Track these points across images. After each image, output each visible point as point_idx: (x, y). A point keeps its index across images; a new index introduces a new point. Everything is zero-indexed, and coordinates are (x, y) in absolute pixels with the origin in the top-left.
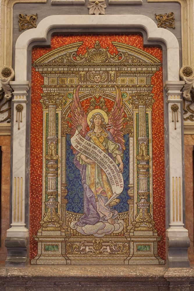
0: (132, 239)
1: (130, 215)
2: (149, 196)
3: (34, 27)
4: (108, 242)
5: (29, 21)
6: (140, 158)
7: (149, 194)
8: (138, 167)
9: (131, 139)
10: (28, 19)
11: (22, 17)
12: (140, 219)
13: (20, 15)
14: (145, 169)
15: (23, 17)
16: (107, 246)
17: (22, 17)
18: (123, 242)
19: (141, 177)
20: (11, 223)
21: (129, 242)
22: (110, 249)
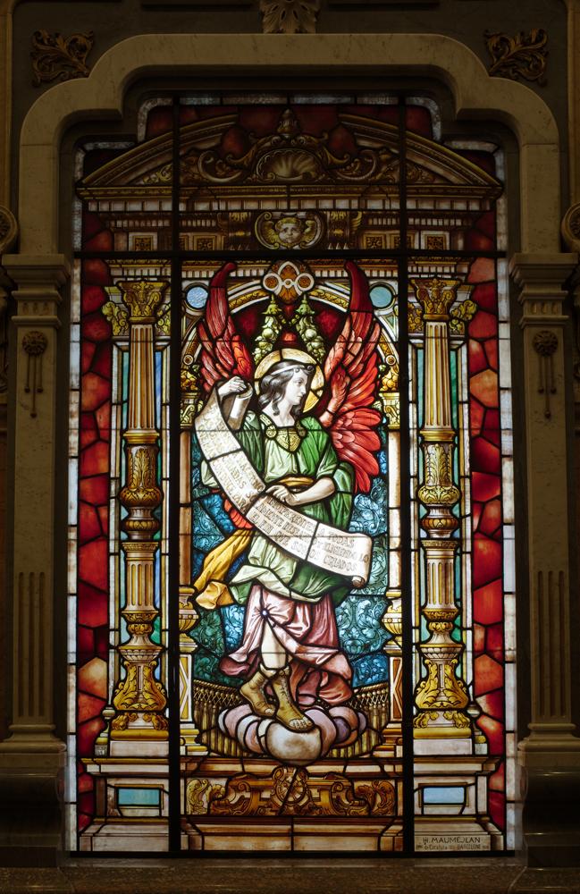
3: (82, 73)
5: (66, 52)
10: (62, 46)
11: (42, 42)
13: (38, 34)
15: (46, 42)
17: (42, 42)
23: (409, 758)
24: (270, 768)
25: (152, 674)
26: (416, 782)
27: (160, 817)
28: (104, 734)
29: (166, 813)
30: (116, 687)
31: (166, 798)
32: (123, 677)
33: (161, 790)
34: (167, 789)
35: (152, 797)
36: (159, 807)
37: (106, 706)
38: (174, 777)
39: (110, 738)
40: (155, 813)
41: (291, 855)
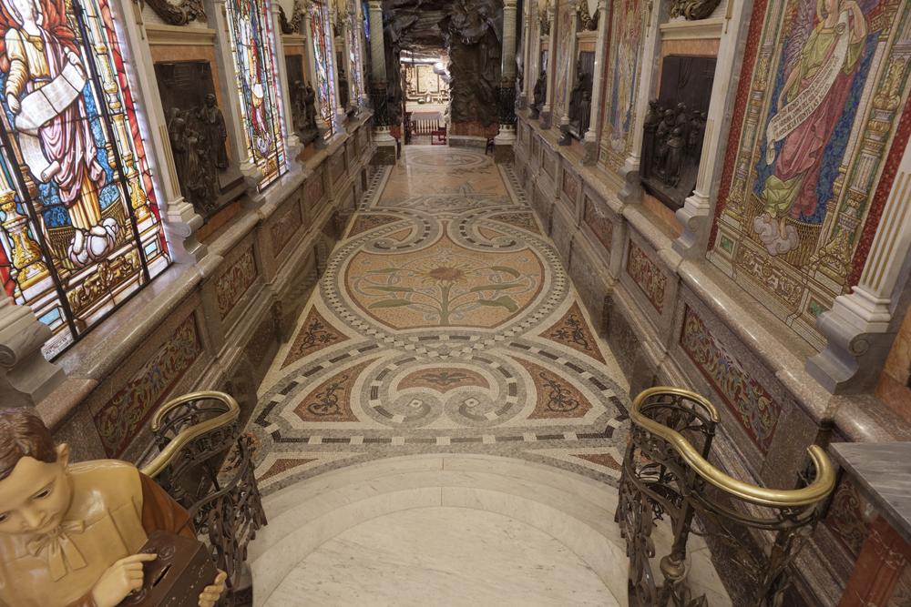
0: (809, 284)
1: (822, 234)
2: (864, 204)
4: (779, 270)
6: (879, 102)
7: (867, 199)
8: (867, 128)
9: (881, 44)
12: (833, 250)
14: (879, 135)
16: (776, 276)
18: (796, 282)
19: (866, 153)
20: (694, 189)
21: (805, 286)
22: (779, 285)
23: (137, 236)
24: (94, 268)
25: (28, 236)
26: (143, 245)
27: (64, 323)
28: (17, 290)
29: (64, 319)
30: (12, 254)
31: (61, 309)
32: (13, 245)
33: (57, 306)
34: (60, 304)
35: (54, 314)
36: (61, 317)
37: (11, 269)
38: (62, 296)
39: (21, 290)
40: (60, 322)
41: (117, 308)
